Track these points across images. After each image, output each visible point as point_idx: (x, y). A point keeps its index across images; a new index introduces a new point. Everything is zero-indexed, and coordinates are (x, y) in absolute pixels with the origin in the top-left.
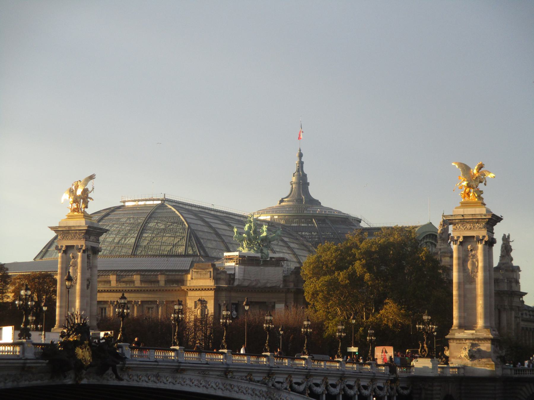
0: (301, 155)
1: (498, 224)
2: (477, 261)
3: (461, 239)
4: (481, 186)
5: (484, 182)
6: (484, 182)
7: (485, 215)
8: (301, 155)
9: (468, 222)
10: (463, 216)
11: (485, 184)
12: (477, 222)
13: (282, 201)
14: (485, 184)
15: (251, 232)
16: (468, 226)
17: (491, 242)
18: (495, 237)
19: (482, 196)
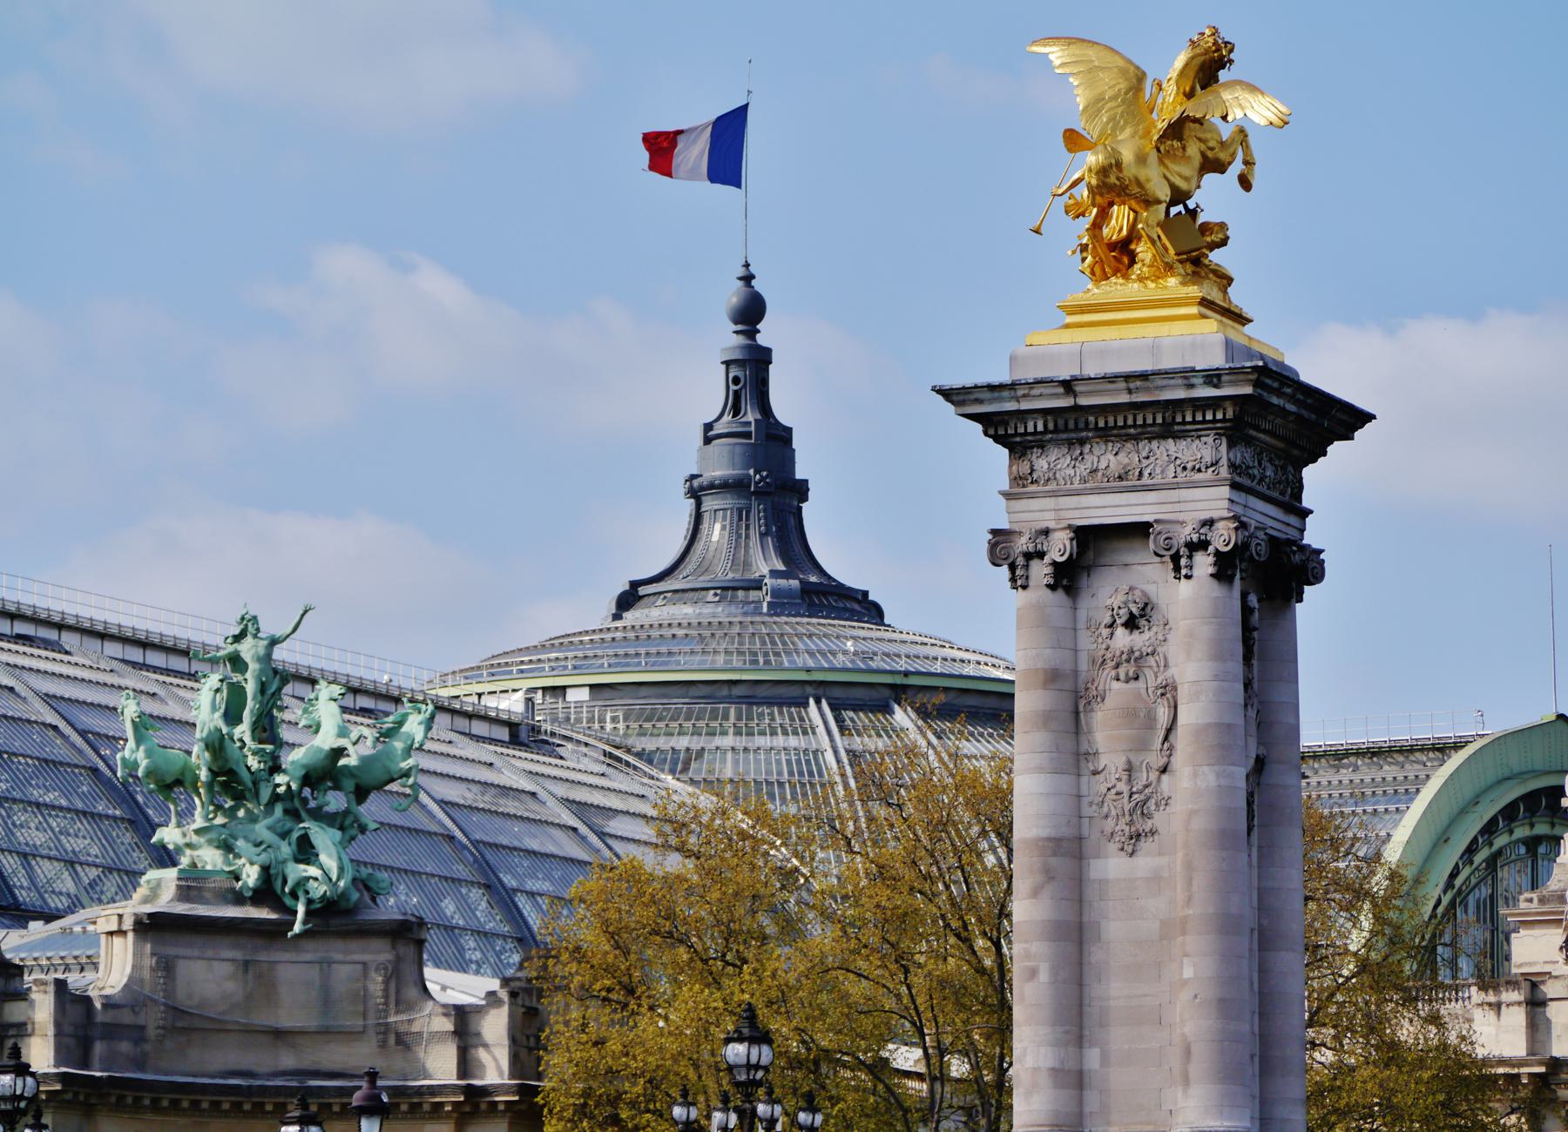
0: (750, 312)
1: (1337, 449)
2: (1168, 690)
3: (1060, 547)
4: (1214, 198)
5: (1236, 168)
6: (1236, 168)
7: (1213, 377)
8: (750, 312)
9: (1105, 434)
10: (1068, 386)
11: (1245, 182)
12: (1168, 432)
13: (628, 600)
14: (1245, 182)
15: (243, 730)
16: (1109, 458)
17: (1272, 573)
18: (1311, 538)
19: (1216, 257)
